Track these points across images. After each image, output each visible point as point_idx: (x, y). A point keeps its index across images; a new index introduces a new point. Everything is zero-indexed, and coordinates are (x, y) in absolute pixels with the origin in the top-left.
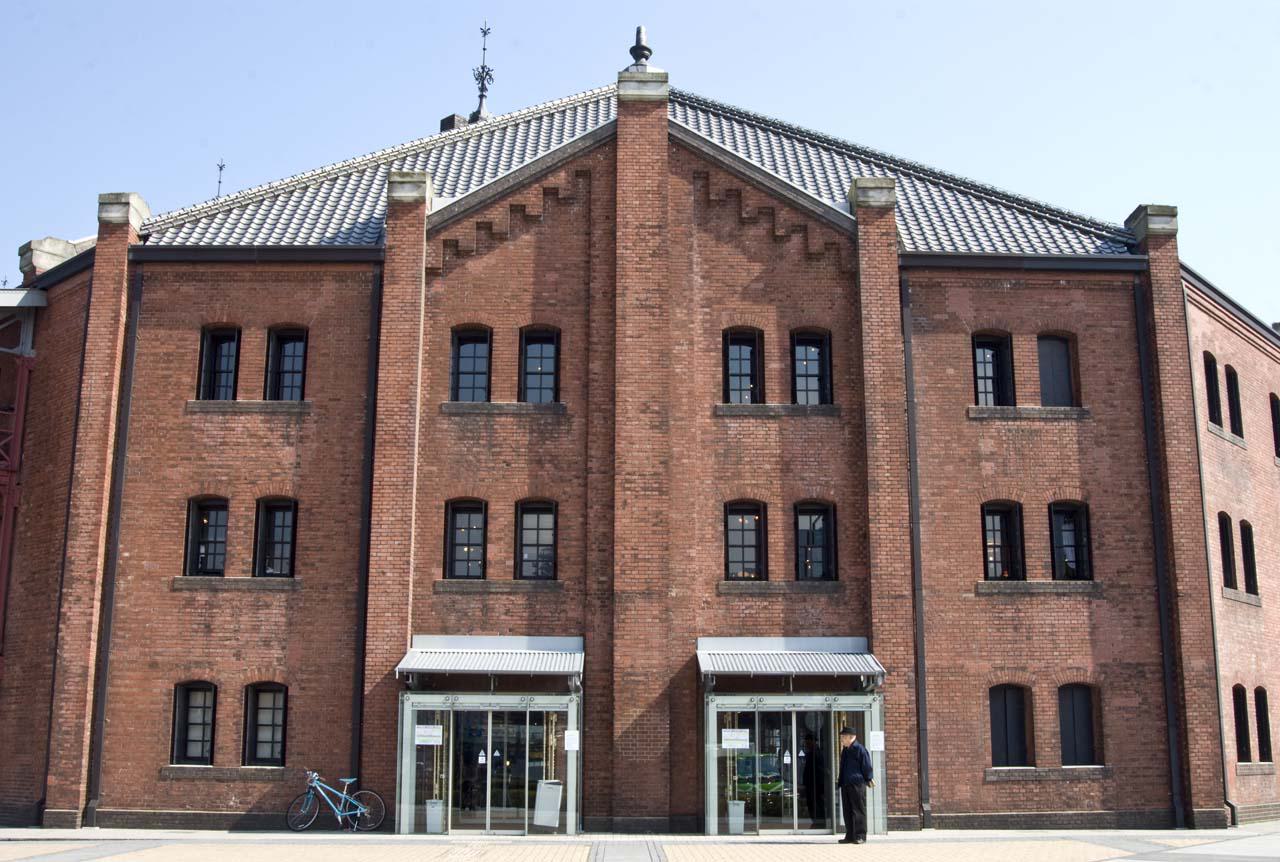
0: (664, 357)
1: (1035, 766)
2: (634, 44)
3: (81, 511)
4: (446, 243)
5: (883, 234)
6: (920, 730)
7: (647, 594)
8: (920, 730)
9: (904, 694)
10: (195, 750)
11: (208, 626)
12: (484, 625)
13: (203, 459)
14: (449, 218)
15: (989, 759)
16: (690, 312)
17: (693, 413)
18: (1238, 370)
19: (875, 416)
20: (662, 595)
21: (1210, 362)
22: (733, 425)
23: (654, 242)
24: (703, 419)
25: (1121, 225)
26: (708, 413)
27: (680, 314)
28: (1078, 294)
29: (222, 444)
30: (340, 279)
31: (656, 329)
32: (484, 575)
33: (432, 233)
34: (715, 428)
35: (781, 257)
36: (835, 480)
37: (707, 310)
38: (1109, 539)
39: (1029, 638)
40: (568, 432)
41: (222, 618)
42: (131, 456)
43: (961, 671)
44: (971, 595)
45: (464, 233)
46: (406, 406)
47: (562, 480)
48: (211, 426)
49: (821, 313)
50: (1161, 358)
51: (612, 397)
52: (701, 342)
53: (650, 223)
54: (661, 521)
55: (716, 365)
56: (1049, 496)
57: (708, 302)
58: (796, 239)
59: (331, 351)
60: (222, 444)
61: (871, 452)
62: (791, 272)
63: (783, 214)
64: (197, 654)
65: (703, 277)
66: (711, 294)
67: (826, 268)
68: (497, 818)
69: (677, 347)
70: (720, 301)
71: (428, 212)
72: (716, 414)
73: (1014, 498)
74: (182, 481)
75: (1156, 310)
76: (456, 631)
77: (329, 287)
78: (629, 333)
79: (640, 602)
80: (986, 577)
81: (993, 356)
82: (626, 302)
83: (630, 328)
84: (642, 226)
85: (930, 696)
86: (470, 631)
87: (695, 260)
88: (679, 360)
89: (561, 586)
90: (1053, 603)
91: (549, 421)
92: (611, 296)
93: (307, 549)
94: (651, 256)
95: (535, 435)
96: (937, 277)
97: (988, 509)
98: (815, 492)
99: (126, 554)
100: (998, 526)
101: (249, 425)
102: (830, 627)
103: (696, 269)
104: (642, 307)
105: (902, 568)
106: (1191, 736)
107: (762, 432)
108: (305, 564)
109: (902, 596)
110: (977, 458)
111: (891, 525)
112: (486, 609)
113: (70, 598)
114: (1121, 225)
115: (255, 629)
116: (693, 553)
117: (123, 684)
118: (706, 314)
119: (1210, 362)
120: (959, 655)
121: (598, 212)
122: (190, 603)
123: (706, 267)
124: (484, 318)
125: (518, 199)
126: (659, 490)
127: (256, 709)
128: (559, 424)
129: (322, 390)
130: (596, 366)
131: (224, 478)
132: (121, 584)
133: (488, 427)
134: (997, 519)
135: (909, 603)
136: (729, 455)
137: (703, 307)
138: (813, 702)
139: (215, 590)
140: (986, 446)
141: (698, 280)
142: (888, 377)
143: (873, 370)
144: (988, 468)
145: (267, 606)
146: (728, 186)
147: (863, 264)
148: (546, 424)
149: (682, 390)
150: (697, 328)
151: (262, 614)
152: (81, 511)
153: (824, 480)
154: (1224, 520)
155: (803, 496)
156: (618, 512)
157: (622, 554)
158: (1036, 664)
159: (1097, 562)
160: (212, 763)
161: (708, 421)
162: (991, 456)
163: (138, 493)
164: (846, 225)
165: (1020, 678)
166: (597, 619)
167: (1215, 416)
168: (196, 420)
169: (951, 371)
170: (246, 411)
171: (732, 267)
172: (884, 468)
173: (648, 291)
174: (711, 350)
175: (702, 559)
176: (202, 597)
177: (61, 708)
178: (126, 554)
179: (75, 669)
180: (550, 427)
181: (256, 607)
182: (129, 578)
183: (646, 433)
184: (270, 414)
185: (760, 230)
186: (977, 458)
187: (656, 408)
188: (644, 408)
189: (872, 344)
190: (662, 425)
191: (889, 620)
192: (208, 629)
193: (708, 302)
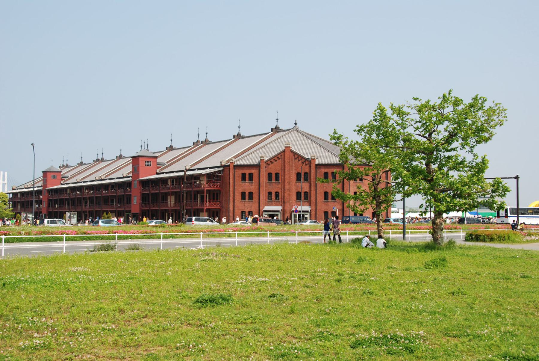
0: (290, 177)
4: (267, 164)
7: (288, 202)
12: (272, 205)
14: (267, 161)
17: (293, 182)
19: (312, 183)
22: (297, 183)
24: (294, 183)
33: (265, 163)
36: (308, 189)
41: (246, 205)
42: (235, 188)
43: (321, 210)
45: (269, 162)
48: (243, 184)
49: (307, 171)
51: (284, 181)
52: (294, 174)
54: (289, 194)
63: (303, 160)
64: (243, 208)
72: (296, 182)
82: (286, 170)
83: (286, 173)
85: (317, 212)
90: (331, 203)
92: (284, 170)
96: (320, 166)
98: (306, 191)
110: (323, 187)
112: (272, 203)
115: (249, 206)
117: (236, 211)
121: (283, 160)
124: (271, 172)
125: (274, 158)
130: (283, 177)
132: (235, 201)
139: (245, 202)
141: (294, 167)
142: (314, 179)
143: (312, 178)
144: (325, 188)
150: (294, 173)
153: (306, 189)
157: (285, 198)
162: (325, 187)
163: (236, 191)
165: (327, 211)
166: (283, 204)
168: (242, 184)
170: (247, 183)
172: (313, 189)
175: (294, 197)
176: (243, 202)
179: (231, 210)
181: (249, 203)
184: (249, 183)
186: (323, 187)
189: (312, 175)
190: (289, 184)
191: (313, 204)
193: (295, 170)
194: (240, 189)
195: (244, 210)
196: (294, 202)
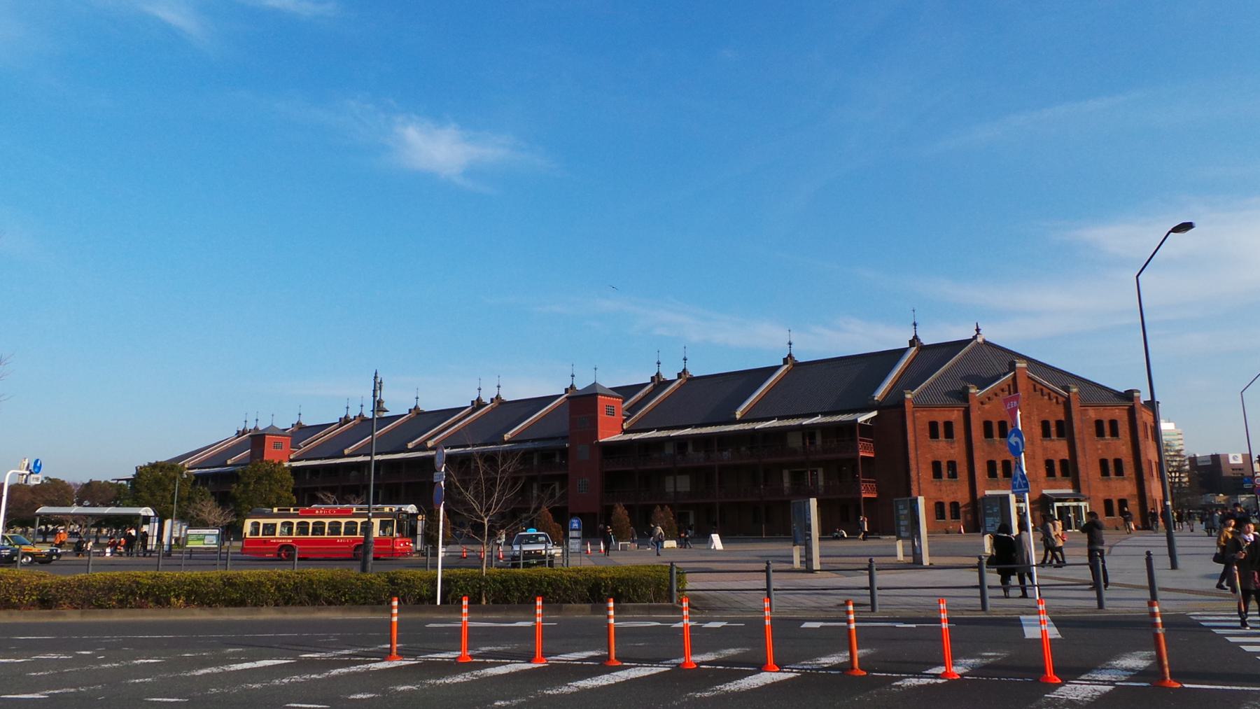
2: (976, 328)
12: (998, 488)
19: (1077, 441)
22: (1045, 442)
24: (1040, 442)
27: (1032, 418)
28: (1117, 411)
30: (958, 410)
48: (933, 443)
57: (1038, 415)
58: (1055, 400)
59: (959, 430)
67: (1061, 407)
68: (825, 556)
72: (1041, 440)
74: (930, 458)
77: (956, 412)
112: (998, 485)
122: (936, 485)
124: (990, 420)
136: (1045, 449)
141: (1035, 410)
144: (1100, 451)
153: (1065, 455)
159: (1125, 472)
162: (1101, 449)
165: (1110, 498)
170: (941, 441)
186: (1098, 449)
192: (940, 490)
194: (928, 456)
196: (1043, 480)
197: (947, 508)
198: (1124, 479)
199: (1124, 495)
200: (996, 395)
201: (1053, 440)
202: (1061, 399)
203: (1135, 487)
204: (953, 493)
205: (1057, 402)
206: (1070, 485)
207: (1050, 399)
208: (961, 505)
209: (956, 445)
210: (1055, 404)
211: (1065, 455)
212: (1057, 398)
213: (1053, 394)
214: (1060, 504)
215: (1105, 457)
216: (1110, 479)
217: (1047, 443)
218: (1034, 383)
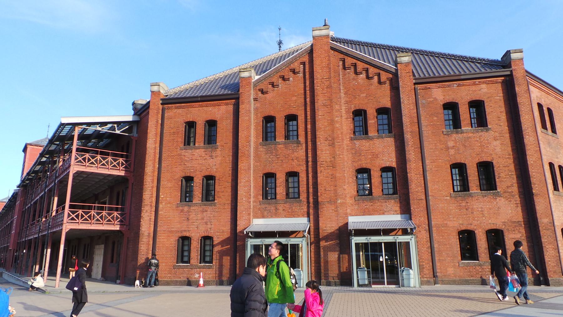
0: (332, 122)
1: (478, 260)
3: (147, 183)
5: (407, 73)
6: (432, 247)
7: (330, 202)
8: (432, 247)
9: (424, 235)
10: (208, 259)
11: (188, 219)
12: (276, 215)
13: (186, 165)
15: (460, 258)
16: (341, 106)
18: (553, 109)
20: (335, 202)
21: (540, 106)
22: (357, 143)
23: (327, 83)
24: (346, 142)
25: (500, 59)
26: (349, 140)
27: (337, 107)
28: (484, 86)
29: (191, 160)
31: (329, 112)
32: (276, 199)
34: (351, 144)
35: (371, 85)
36: (394, 160)
37: (346, 105)
38: (502, 175)
39: (472, 213)
40: (302, 149)
41: (192, 216)
44: (449, 198)
46: (248, 144)
47: (300, 165)
48: (188, 153)
49: (386, 102)
50: (520, 106)
53: (325, 77)
54: (333, 177)
55: (350, 123)
56: (477, 160)
58: (376, 78)
60: (191, 160)
61: (407, 149)
62: (375, 89)
65: (344, 94)
66: (348, 99)
67: (387, 86)
69: (337, 118)
70: (350, 101)
71: (253, 81)
72: (351, 139)
73: (463, 162)
74: (179, 174)
75: (517, 89)
76: (267, 217)
78: (320, 114)
79: (327, 205)
80: (454, 191)
81: (452, 112)
84: (323, 79)
85: (435, 235)
86: (272, 217)
87: (341, 88)
88: (337, 122)
89: (301, 201)
91: (295, 146)
93: (219, 192)
94: (326, 88)
95: (290, 151)
97: (454, 166)
98: (388, 164)
99: (162, 196)
100: (457, 172)
101: (199, 153)
102: (396, 211)
103: (342, 91)
104: (324, 105)
105: (421, 189)
106: (544, 249)
107: (368, 144)
108: (218, 197)
109: (422, 199)
111: (416, 174)
112: (277, 209)
113: (144, 211)
114: (500, 59)
115: (203, 219)
116: (345, 187)
118: (346, 106)
119: (540, 106)
120: (445, 220)
122: (182, 211)
123: (345, 90)
124: (272, 114)
126: (333, 168)
127: (205, 245)
128: (298, 147)
129: (222, 140)
131: (192, 170)
132: (161, 206)
133: (275, 149)
134: (457, 170)
135: (424, 202)
136: (357, 153)
137: (345, 104)
138: (389, 239)
140: (451, 144)
141: (342, 95)
142: (412, 123)
144: (452, 152)
145: (206, 211)
146: (352, 62)
147: (401, 84)
148: (294, 147)
149: (339, 132)
150: (343, 111)
151: (205, 214)
152: (147, 183)
153: (391, 160)
154: (551, 165)
155: (383, 166)
156: (319, 175)
158: (476, 222)
159: (498, 184)
160: (189, 263)
161: (349, 142)
164: (394, 71)
165: (470, 228)
167: (544, 126)
169: (435, 118)
170: (199, 148)
171: (354, 89)
172: (412, 154)
173: (326, 100)
174: (349, 118)
176: (186, 209)
177: (141, 247)
178: (162, 196)
179: (146, 234)
180: (296, 148)
182: (163, 204)
183: (327, 148)
185: (363, 76)
186: (448, 148)
187: (330, 139)
188: (326, 139)
190: (332, 145)
191: (417, 207)
195: (187, 234)
196: (350, 201)
197: (195, 246)
198: (498, 195)
199: (497, 223)
200: (284, 78)
201: (372, 139)
202: (384, 76)
203: (519, 209)
204: (206, 223)
205: (380, 82)
206: (398, 209)
207: (368, 77)
208: (216, 241)
209: (218, 152)
210: (377, 84)
211: (391, 160)
212: (379, 75)
213: (372, 70)
214: (362, 240)
215: (460, 159)
216: (471, 196)
217: (363, 144)
218: (342, 56)
